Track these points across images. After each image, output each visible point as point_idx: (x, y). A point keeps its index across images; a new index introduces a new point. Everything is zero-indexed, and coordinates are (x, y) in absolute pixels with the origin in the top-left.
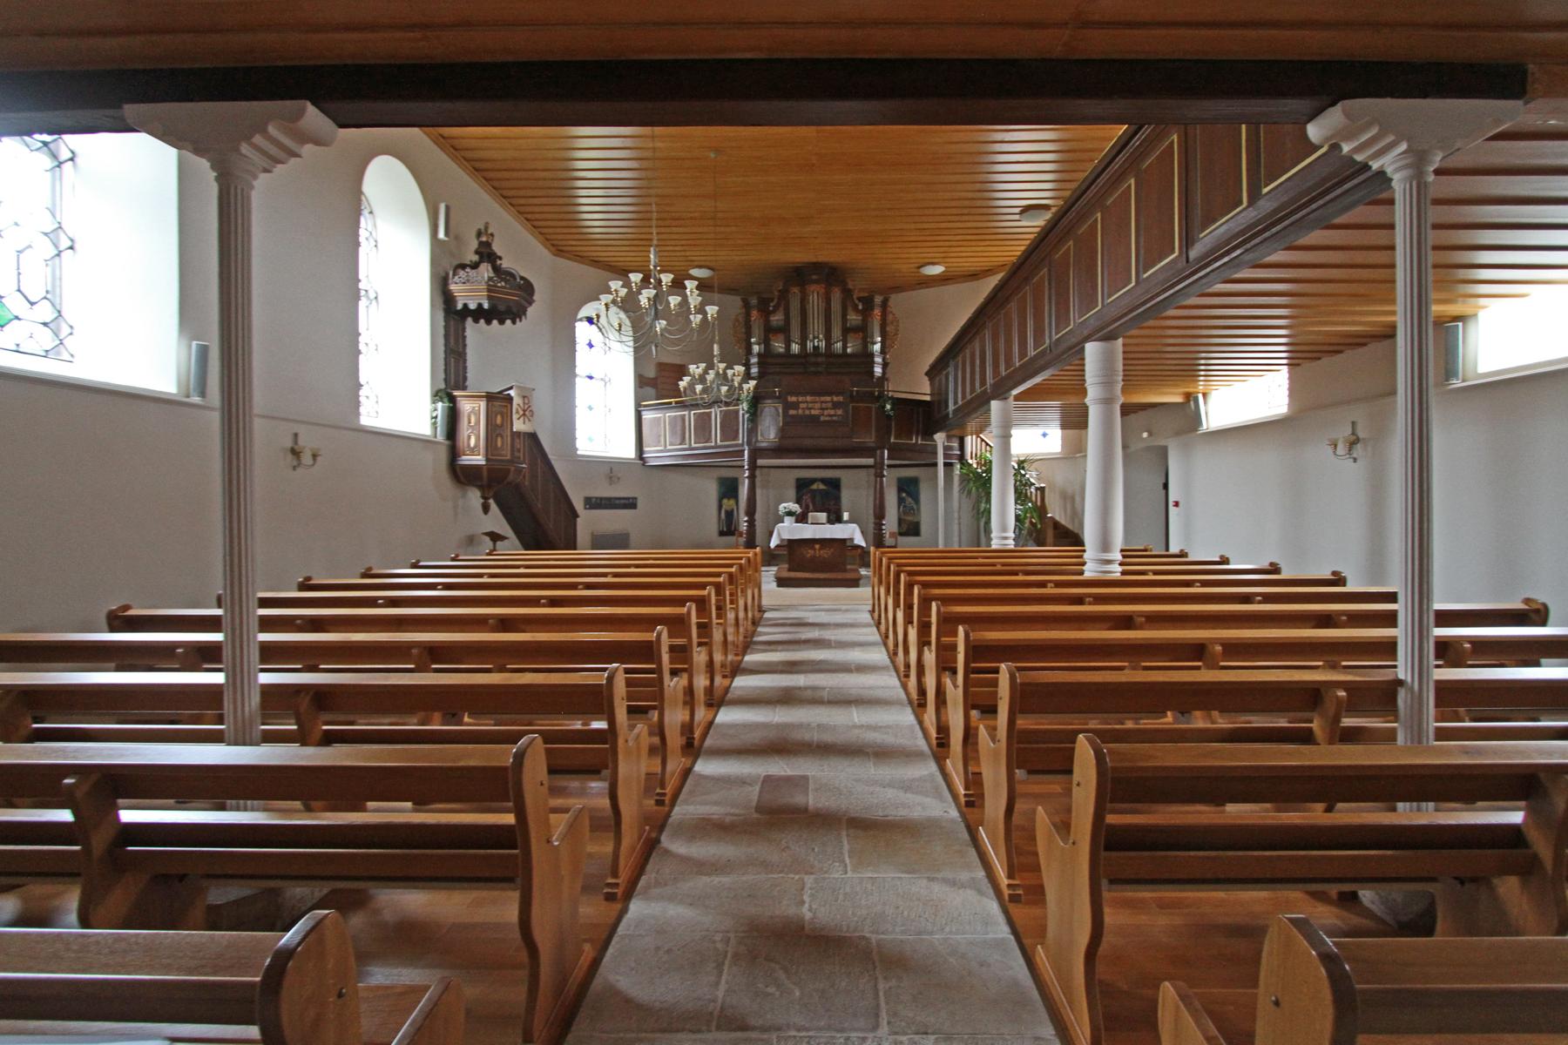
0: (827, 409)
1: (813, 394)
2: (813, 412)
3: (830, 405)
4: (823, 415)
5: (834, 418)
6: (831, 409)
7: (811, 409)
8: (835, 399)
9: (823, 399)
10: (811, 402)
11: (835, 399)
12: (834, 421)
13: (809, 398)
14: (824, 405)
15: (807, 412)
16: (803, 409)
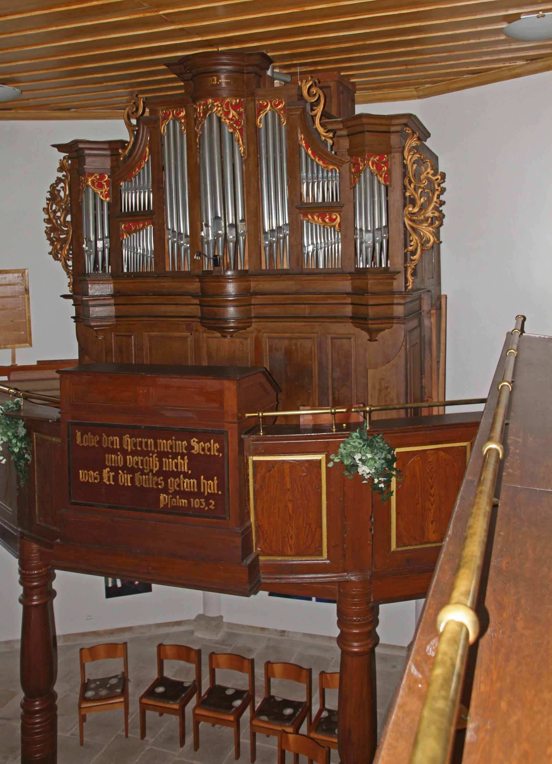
0: (176, 475)
1: (134, 432)
2: (141, 480)
3: (184, 464)
4: (165, 491)
5: (196, 503)
6: (186, 476)
7: (132, 471)
8: (197, 446)
9: (165, 444)
10: (134, 453)
11: (197, 446)
12: (200, 513)
13: (128, 442)
14: (170, 464)
15: (125, 479)
16: (115, 469)
